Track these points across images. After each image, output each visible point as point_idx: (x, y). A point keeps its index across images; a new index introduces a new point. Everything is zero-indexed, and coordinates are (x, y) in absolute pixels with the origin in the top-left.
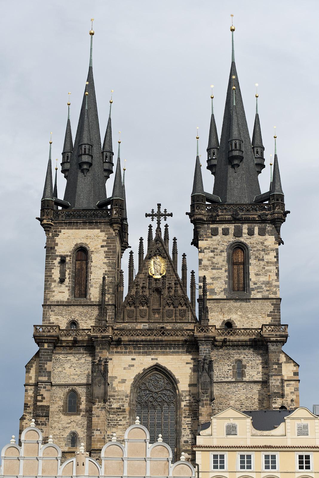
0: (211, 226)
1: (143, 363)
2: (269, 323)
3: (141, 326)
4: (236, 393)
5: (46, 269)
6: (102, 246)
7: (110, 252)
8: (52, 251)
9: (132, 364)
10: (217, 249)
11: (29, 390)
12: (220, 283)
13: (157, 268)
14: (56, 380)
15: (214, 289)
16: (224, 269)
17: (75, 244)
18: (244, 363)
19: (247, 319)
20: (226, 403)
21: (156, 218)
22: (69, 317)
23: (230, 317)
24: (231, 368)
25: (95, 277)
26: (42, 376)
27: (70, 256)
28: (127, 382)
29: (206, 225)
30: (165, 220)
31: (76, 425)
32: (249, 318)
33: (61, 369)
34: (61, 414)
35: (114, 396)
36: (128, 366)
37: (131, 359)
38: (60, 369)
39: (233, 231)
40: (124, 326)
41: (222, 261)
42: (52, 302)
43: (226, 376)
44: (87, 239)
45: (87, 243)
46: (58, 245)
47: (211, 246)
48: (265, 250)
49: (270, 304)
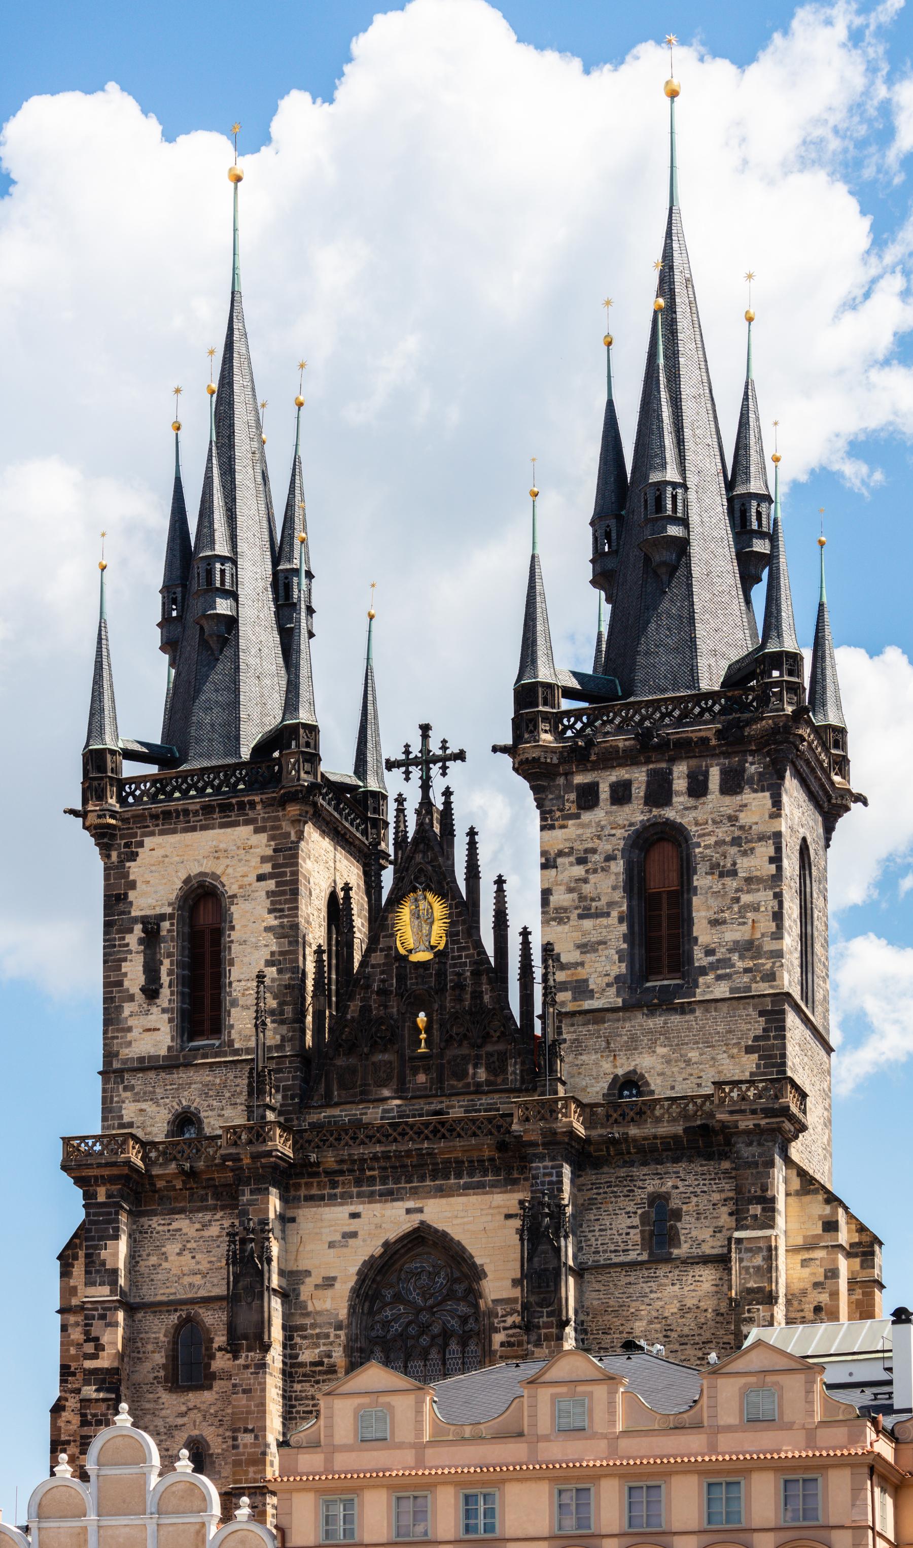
0: (575, 782)
1: (384, 1225)
2: (752, 1074)
3: (377, 1113)
4: (652, 1296)
5: (105, 962)
6: (261, 878)
7: (283, 893)
8: (121, 907)
9: (352, 1229)
10: (594, 851)
11: (72, 1325)
12: (604, 958)
13: (420, 930)
14: (144, 1291)
15: (586, 981)
16: (615, 914)
17: (184, 877)
18: (674, 1203)
19: (683, 1065)
20: (621, 1328)
21: (416, 773)
22: (174, 1104)
23: (633, 1063)
24: (636, 1221)
25: (242, 977)
26: (93, 1284)
27: (171, 916)
28: (337, 1285)
29: (561, 781)
30: (444, 774)
31: (201, 1418)
32: (684, 1062)
33: (155, 1258)
34: (160, 1389)
35: (303, 1328)
36: (338, 1237)
37: (347, 1216)
38: (153, 1260)
39: (643, 787)
40: (329, 1117)
41: (610, 890)
42: (125, 1061)
43: (622, 1247)
44: (218, 858)
45: (218, 872)
46: (138, 884)
47: (578, 846)
48: (742, 841)
49: (754, 1014)
